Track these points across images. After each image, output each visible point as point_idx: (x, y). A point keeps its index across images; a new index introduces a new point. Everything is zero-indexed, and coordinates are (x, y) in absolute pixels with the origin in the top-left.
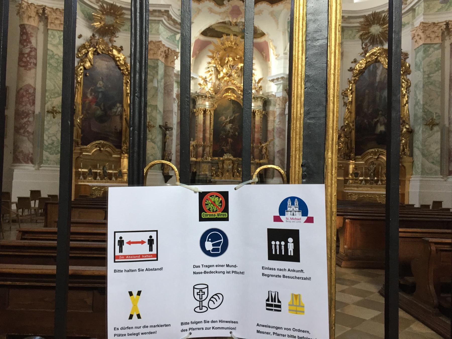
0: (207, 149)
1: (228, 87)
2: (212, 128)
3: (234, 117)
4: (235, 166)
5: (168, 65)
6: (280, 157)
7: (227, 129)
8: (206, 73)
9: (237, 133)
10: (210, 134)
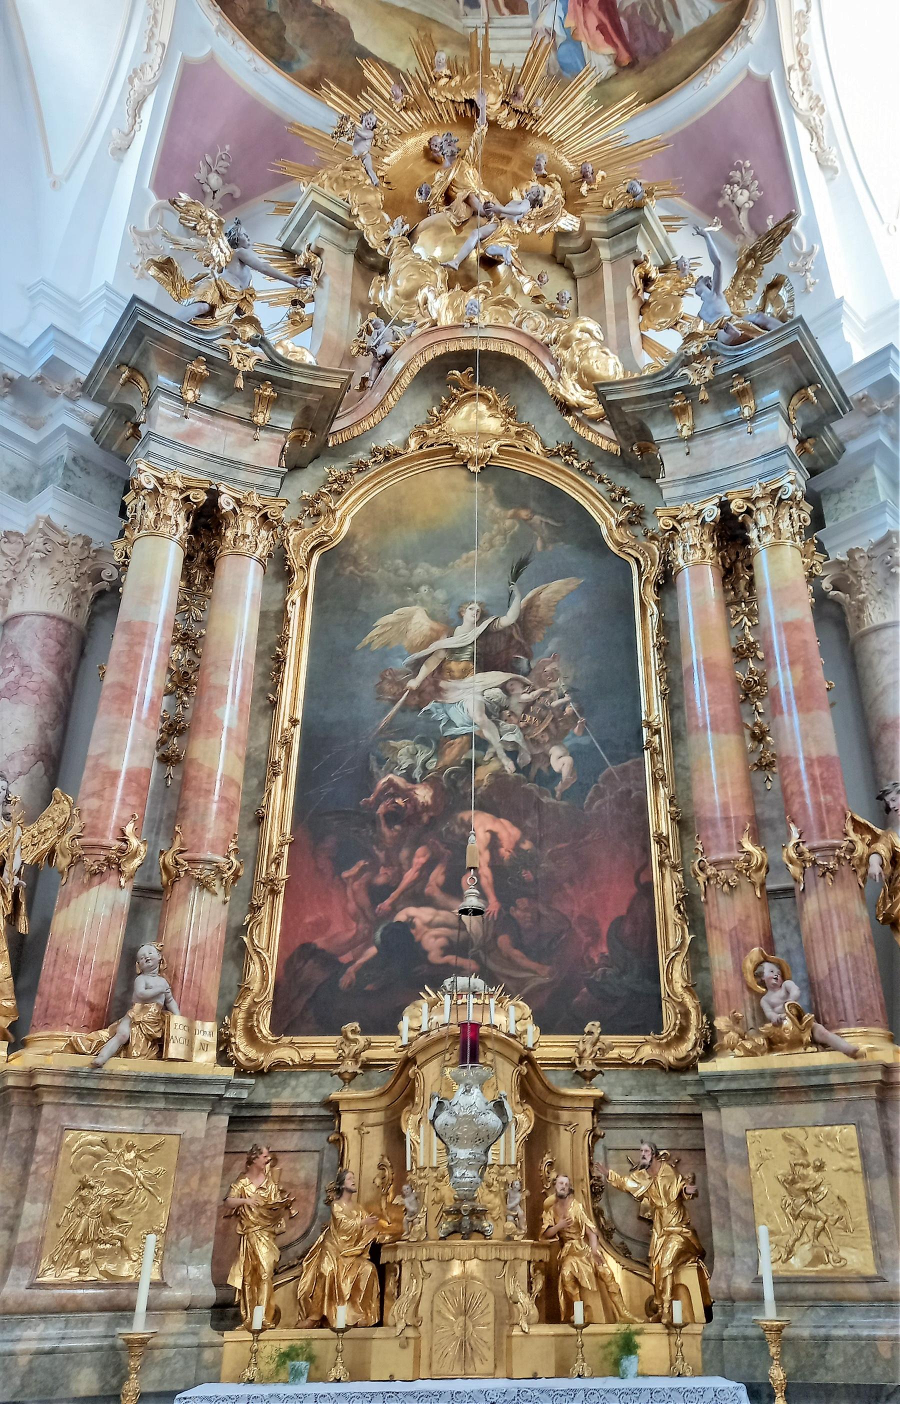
7: (456, 715)
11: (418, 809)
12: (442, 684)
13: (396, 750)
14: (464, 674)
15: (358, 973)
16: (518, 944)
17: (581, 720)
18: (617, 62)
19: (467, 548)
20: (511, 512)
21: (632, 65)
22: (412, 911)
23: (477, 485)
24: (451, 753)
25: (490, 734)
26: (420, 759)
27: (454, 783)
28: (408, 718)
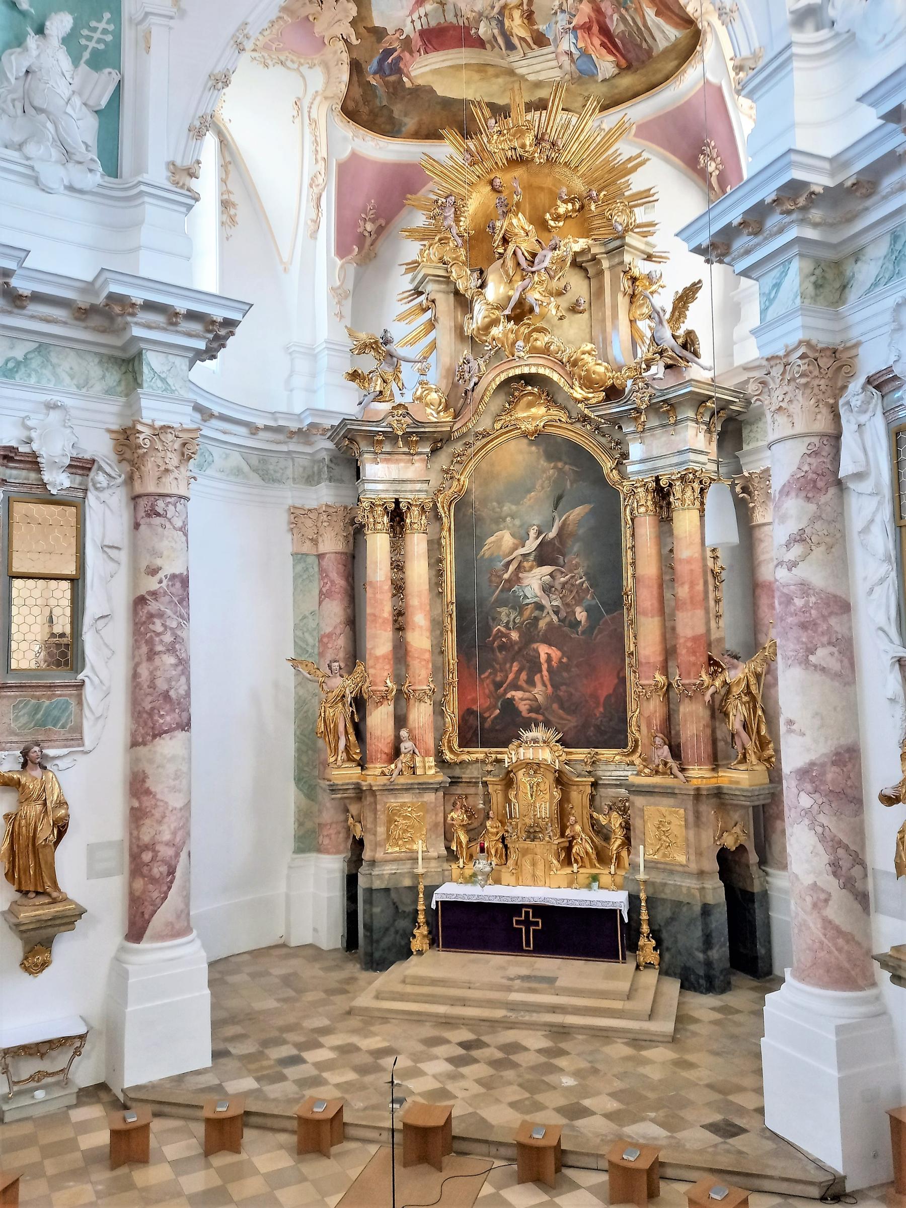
1: (511, 373)
2: (450, 593)
3: (561, 529)
4: (574, 795)
9: (581, 615)
11: (512, 643)
12: (521, 575)
13: (500, 613)
14: (531, 569)
15: (493, 722)
16: (562, 707)
17: (591, 590)
19: (529, 491)
20: (552, 465)
21: (629, 67)
22: (513, 693)
24: (527, 613)
25: (544, 601)
26: (512, 617)
27: (529, 629)
28: (505, 595)
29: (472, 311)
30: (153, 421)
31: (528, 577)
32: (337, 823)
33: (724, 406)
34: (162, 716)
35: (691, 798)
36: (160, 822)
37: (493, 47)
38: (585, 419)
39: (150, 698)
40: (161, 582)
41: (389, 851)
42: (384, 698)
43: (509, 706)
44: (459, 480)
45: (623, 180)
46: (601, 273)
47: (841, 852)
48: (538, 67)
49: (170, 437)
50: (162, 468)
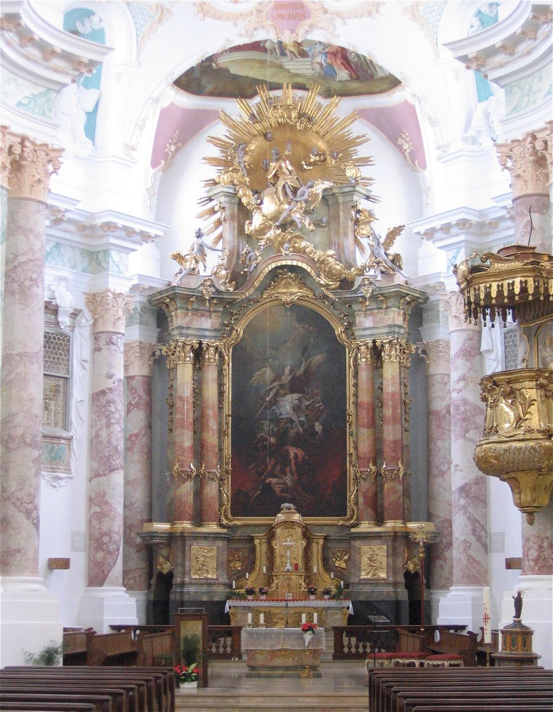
0: (211, 489)
1: (279, 264)
2: (227, 409)
3: (307, 370)
4: (314, 545)
5: (24, 195)
6: (469, 509)
7: (283, 410)
8: (200, 216)
9: (318, 427)
10: (221, 434)
13: (263, 424)
14: (285, 395)
18: (351, 76)
20: (302, 326)
21: (358, 78)
22: (271, 479)
23: (289, 314)
25: (294, 418)
26: (271, 427)
29: (251, 219)
30: (115, 290)
31: (283, 401)
32: (140, 569)
33: (415, 299)
34: (114, 460)
35: (391, 538)
36: (113, 520)
37: (272, 53)
38: (326, 297)
39: (108, 450)
40: (114, 383)
41: (193, 577)
42: (189, 476)
43: (268, 488)
44: (237, 331)
45: (353, 149)
46: (337, 203)
47: (477, 524)
48: (299, 67)
49: (121, 300)
50: (116, 317)
